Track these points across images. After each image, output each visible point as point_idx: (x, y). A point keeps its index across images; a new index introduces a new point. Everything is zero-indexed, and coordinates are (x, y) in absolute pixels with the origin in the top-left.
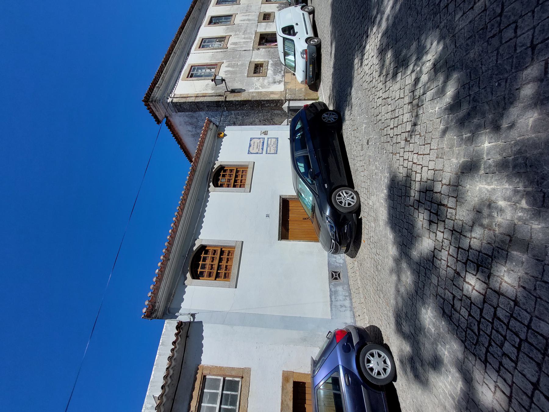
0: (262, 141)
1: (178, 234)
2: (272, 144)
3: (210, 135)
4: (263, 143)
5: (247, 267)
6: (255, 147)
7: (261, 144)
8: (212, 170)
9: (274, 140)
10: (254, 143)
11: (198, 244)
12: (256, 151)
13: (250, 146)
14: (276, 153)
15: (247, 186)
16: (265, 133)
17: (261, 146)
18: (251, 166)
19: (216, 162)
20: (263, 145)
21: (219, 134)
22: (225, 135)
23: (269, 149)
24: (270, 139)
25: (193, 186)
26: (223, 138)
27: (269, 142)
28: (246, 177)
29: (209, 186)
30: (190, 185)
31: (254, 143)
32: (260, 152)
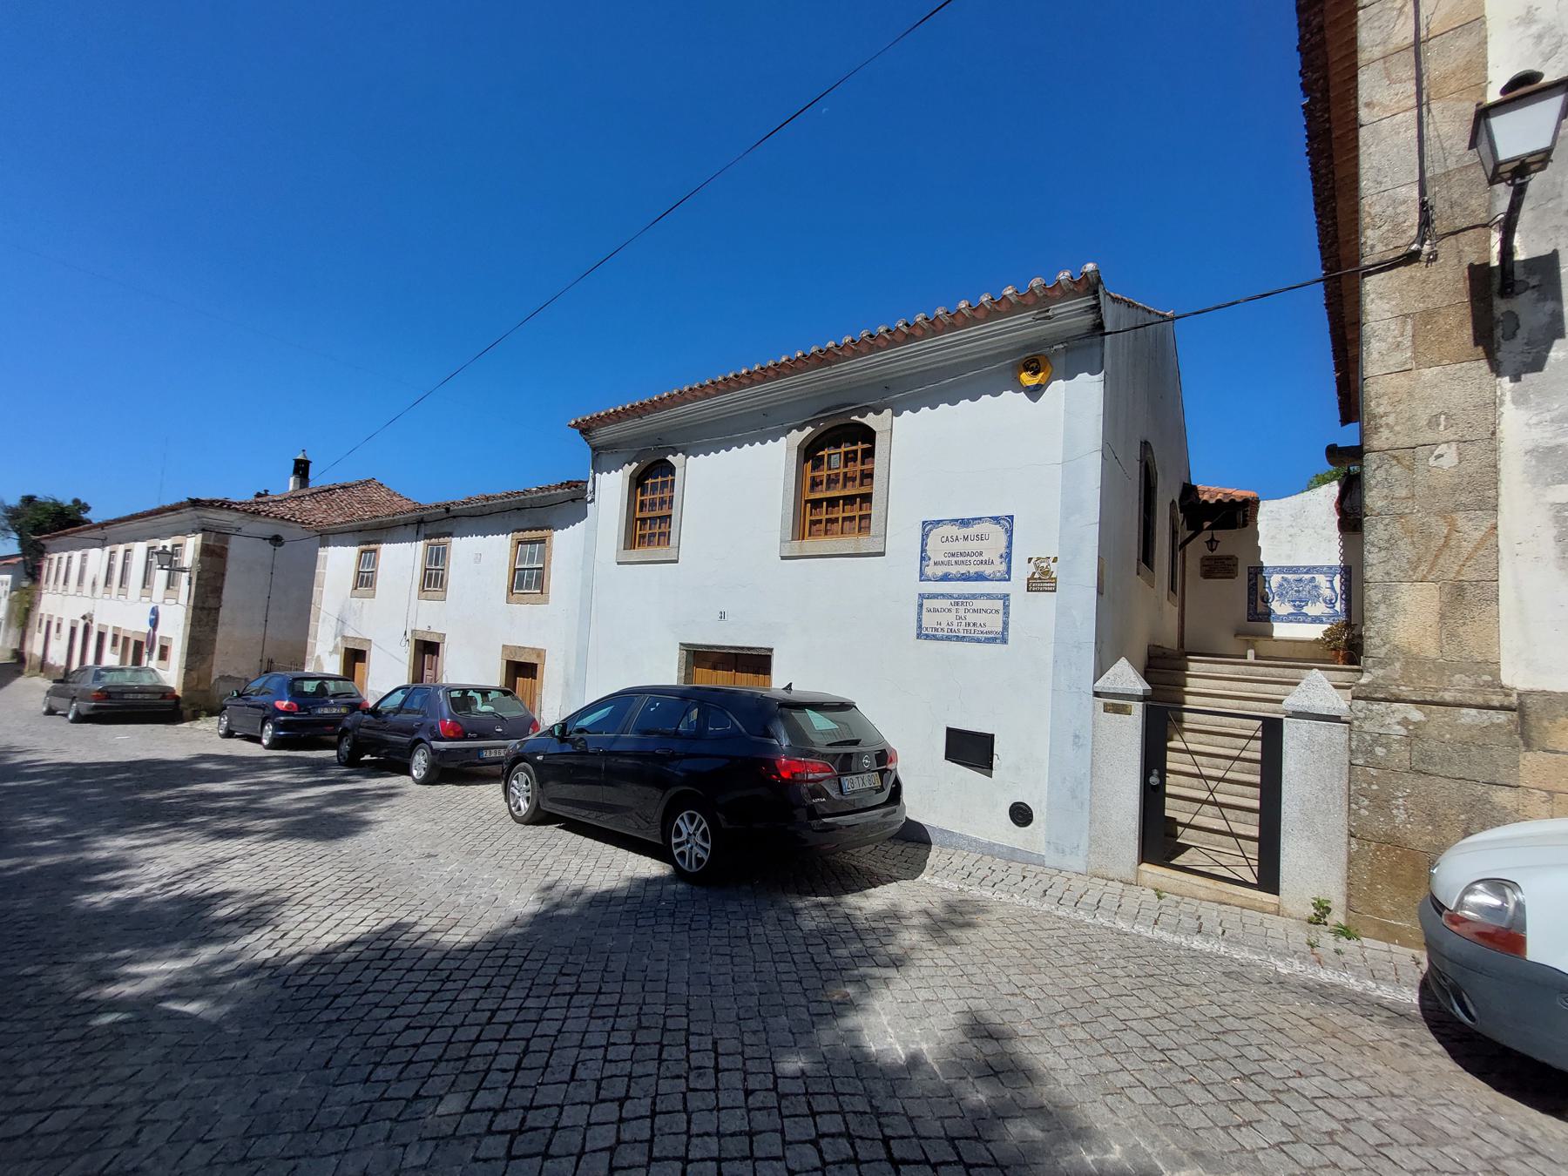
0: (987, 570)
1: (680, 410)
2: (971, 618)
3: (1020, 327)
4: (980, 577)
5: (647, 579)
6: (960, 546)
7: (973, 569)
8: (853, 412)
9: (994, 623)
10: (980, 537)
11: (870, 420)
12: (936, 549)
13: (964, 523)
14: (919, 636)
15: (796, 547)
16: (1041, 581)
17: (963, 569)
18: (865, 543)
19: (888, 412)
20: (965, 578)
21: (1033, 366)
22: (1035, 392)
23: (946, 603)
24: (999, 604)
25: (784, 382)
26: (1018, 387)
27: (978, 604)
28: (851, 532)
29: (801, 428)
30: (778, 375)
31: (980, 537)
32: (929, 571)
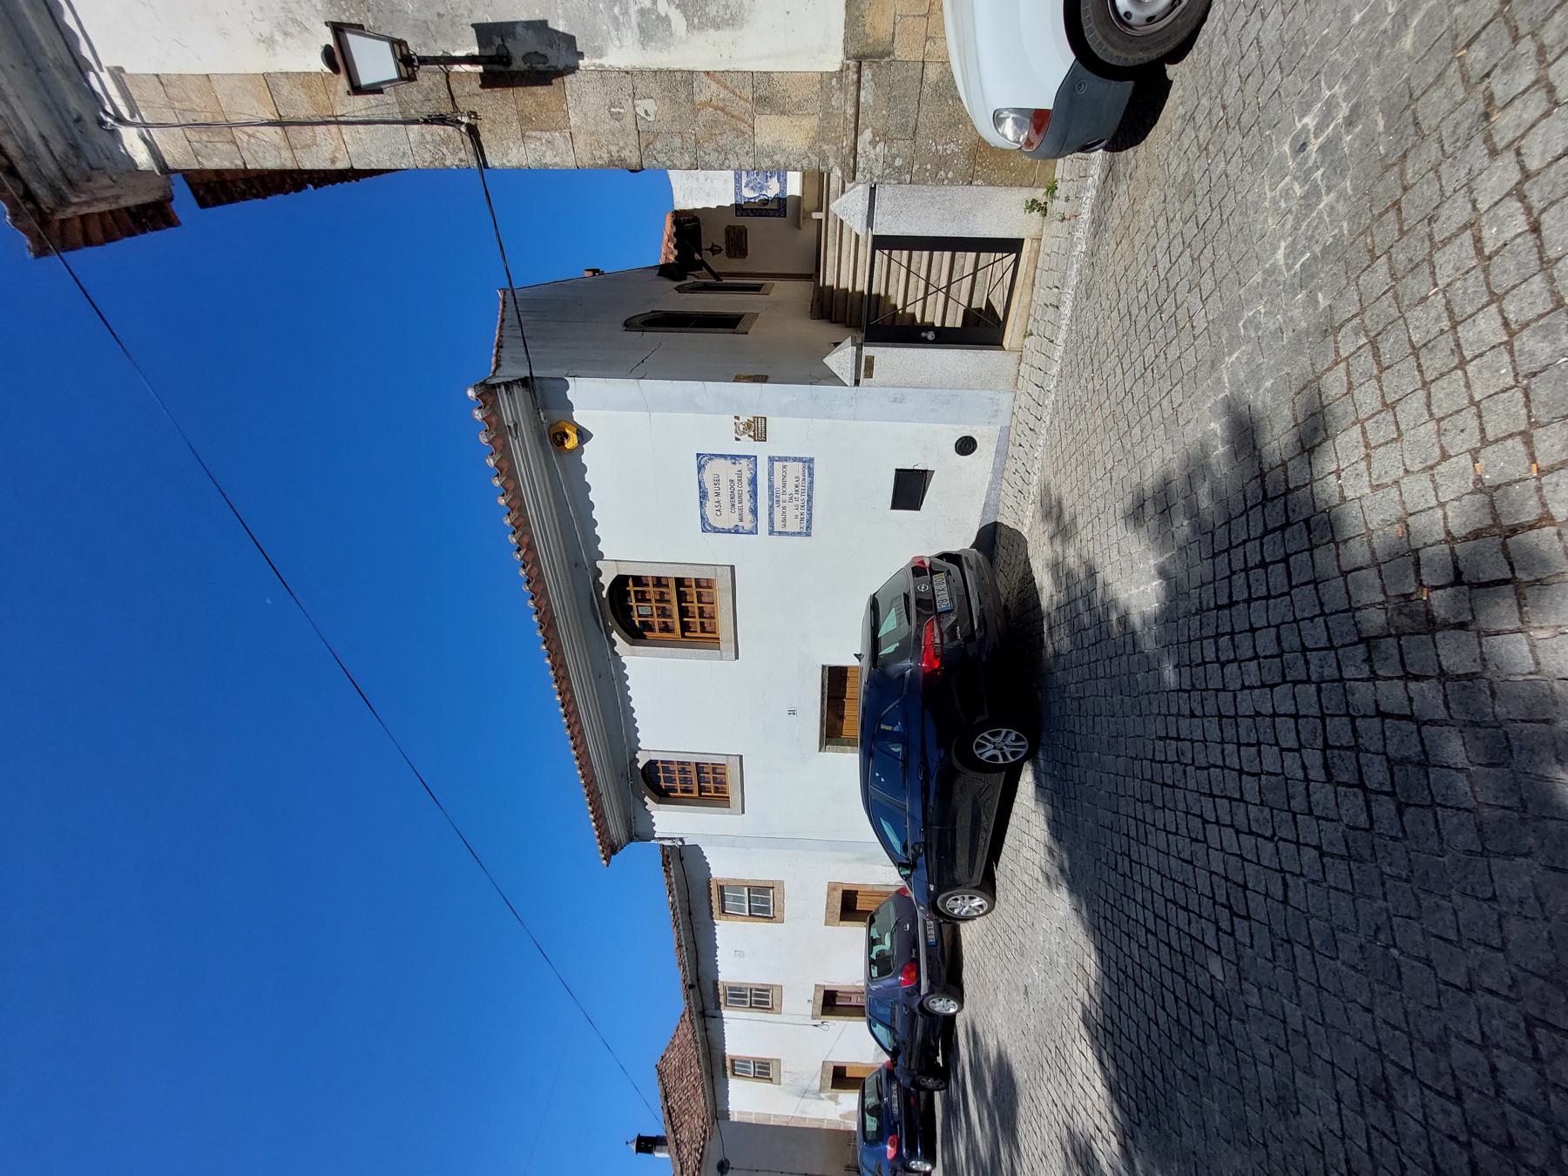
0: (747, 475)
2: (790, 489)
3: (524, 451)
4: (753, 482)
5: (759, 785)
7: (746, 488)
8: (599, 595)
9: (795, 469)
10: (717, 482)
11: (606, 580)
12: (727, 519)
13: (703, 496)
14: (808, 535)
16: (757, 429)
17: (746, 497)
18: (722, 583)
19: (599, 564)
20: (754, 494)
22: (583, 435)
23: (778, 512)
25: (569, 659)
26: (579, 450)
27: (778, 483)
29: (613, 643)
30: (563, 665)
31: (717, 482)
32: (748, 526)
